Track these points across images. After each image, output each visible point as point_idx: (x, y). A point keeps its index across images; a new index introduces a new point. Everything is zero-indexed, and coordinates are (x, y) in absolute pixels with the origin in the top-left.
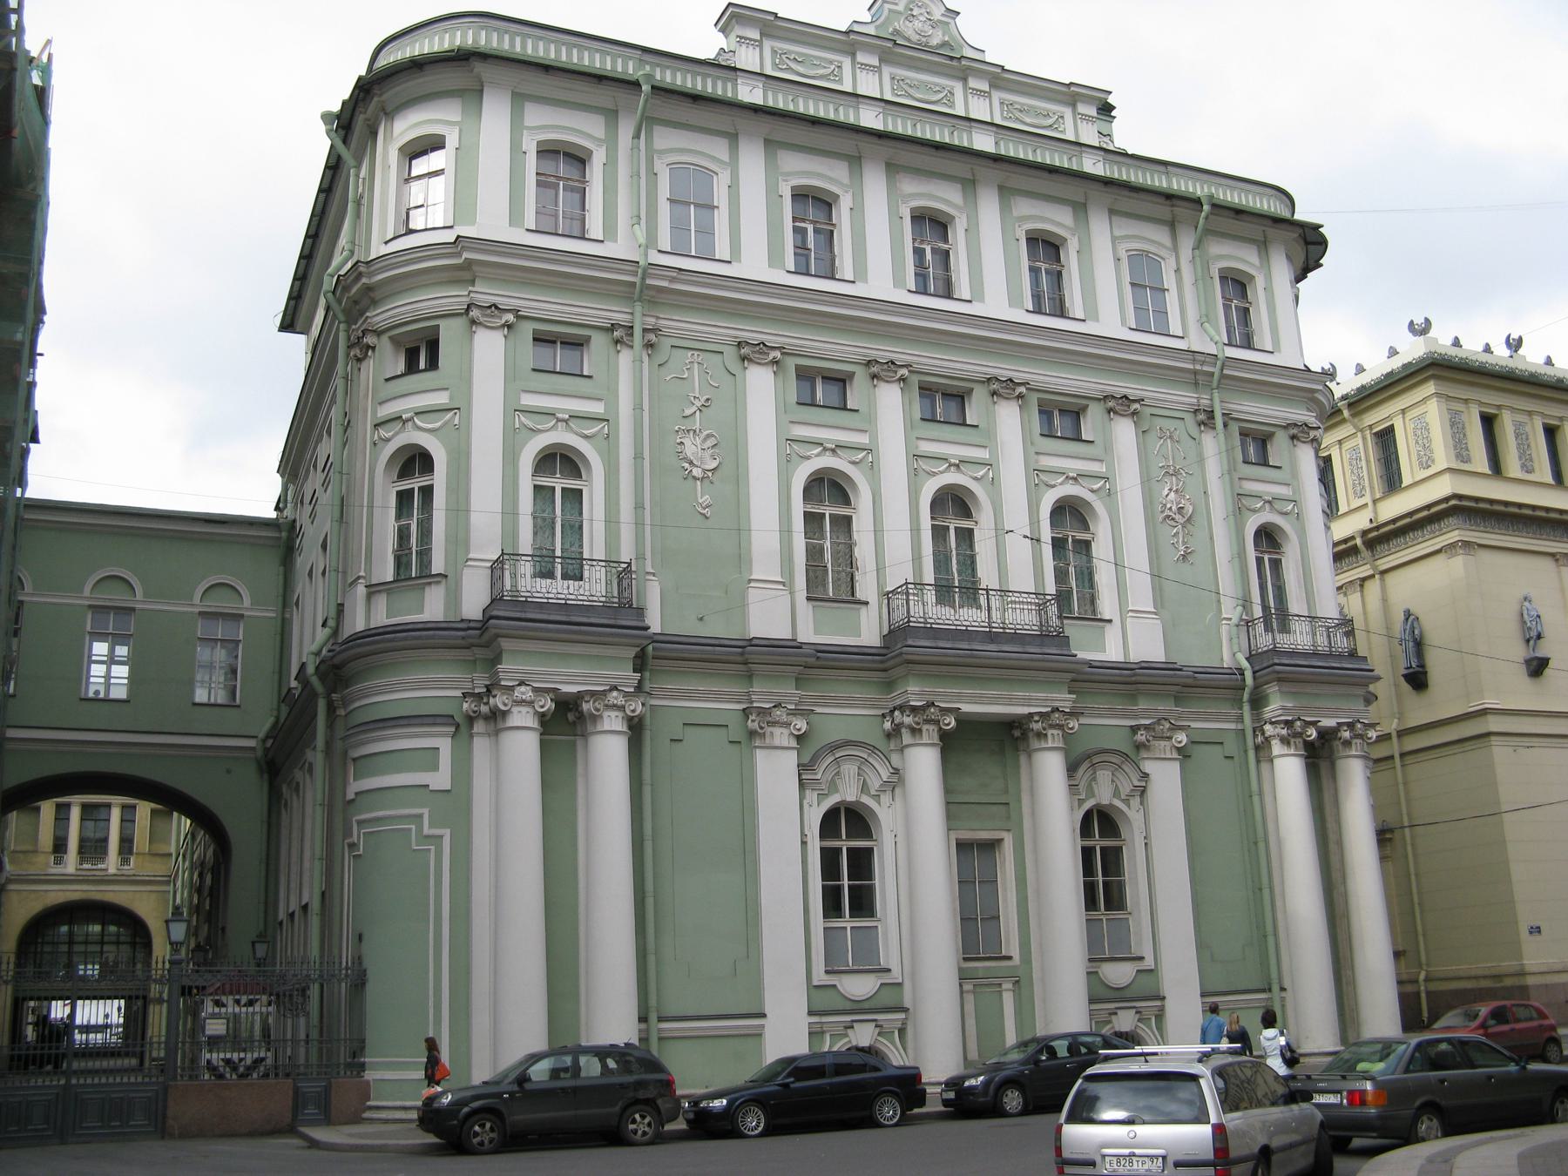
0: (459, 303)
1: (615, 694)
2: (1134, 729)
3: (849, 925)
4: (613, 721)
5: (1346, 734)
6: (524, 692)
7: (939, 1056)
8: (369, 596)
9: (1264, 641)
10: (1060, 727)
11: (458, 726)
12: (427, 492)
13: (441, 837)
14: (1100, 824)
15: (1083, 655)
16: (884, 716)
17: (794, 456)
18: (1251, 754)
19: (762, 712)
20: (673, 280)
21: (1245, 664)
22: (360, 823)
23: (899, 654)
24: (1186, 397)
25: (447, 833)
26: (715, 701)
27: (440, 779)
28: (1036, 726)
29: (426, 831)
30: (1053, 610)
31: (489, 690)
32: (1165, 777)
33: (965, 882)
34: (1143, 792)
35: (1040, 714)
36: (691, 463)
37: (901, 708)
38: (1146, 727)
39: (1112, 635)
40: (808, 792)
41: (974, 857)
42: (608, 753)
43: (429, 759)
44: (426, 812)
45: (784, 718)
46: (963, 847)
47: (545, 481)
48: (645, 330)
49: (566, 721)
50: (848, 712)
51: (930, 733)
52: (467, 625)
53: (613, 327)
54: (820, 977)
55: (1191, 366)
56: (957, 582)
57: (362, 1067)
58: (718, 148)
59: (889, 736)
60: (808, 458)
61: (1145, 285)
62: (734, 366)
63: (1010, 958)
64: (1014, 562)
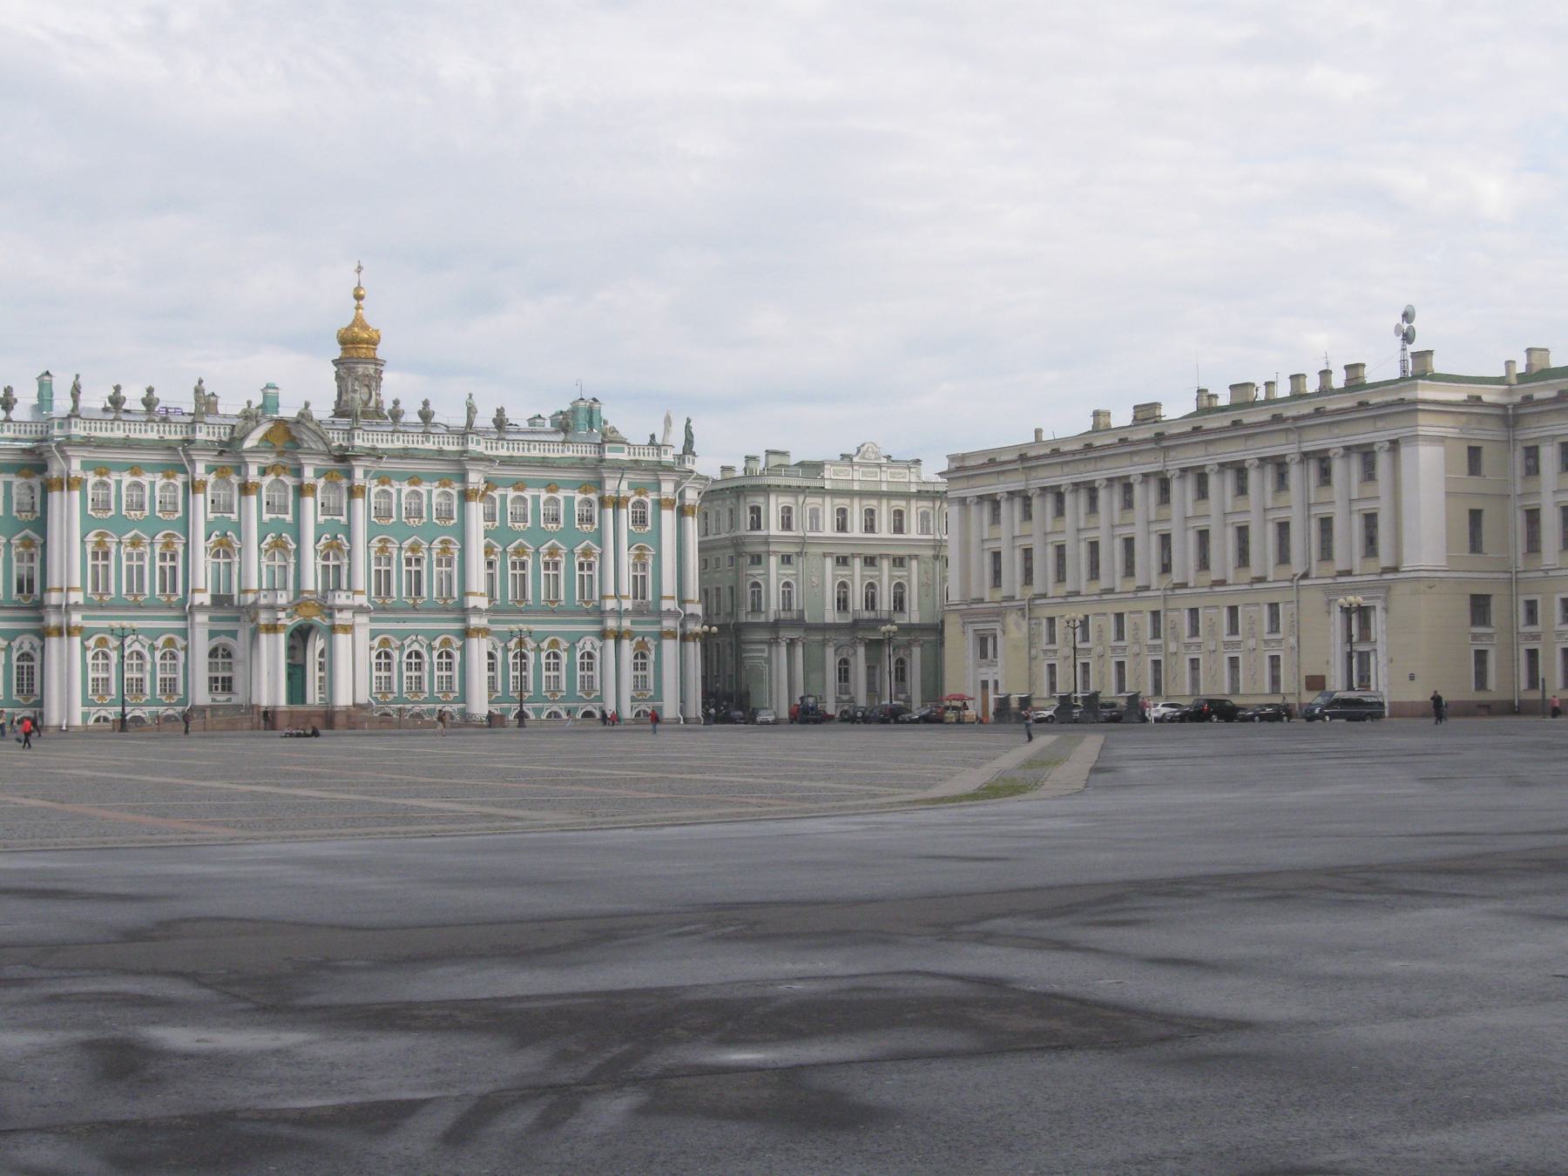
23: (856, 625)
27: (765, 655)
32: (916, 652)
41: (871, 669)
42: (799, 651)
49: (791, 644)
50: (845, 638)
56: (871, 602)
58: (819, 500)
64: (885, 603)
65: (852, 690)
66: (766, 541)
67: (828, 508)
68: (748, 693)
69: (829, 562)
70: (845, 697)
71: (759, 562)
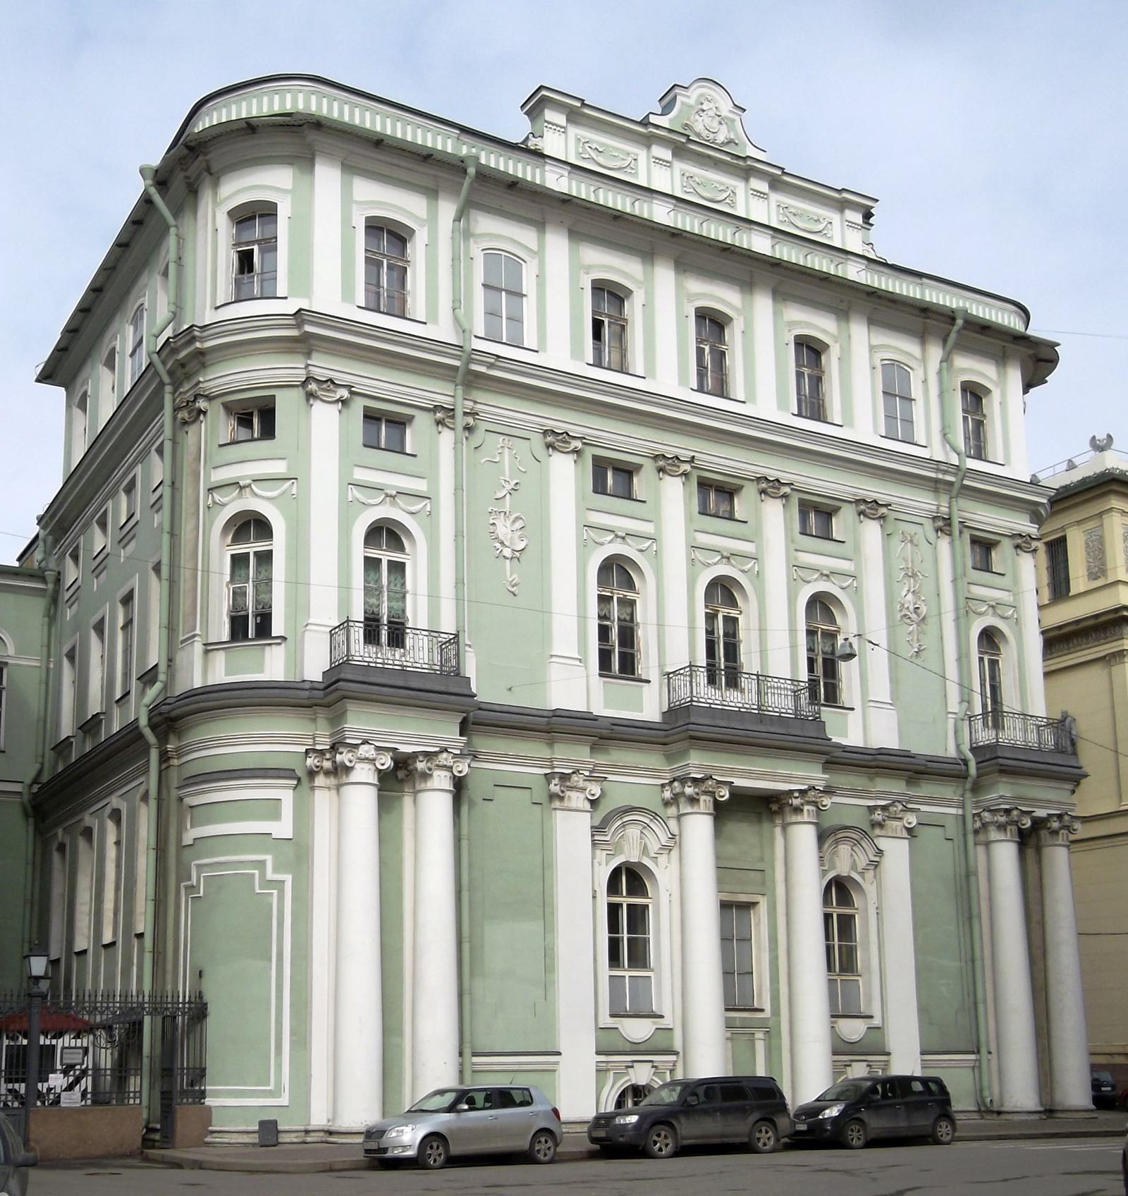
0: (298, 375)
1: (445, 755)
2: (872, 809)
3: (627, 974)
4: (441, 780)
5: (1055, 825)
6: (365, 751)
7: (810, 1080)
8: (206, 652)
9: (985, 736)
10: (815, 803)
11: (299, 780)
12: (265, 558)
13: (283, 882)
14: (839, 890)
15: (835, 739)
16: (663, 786)
17: (590, 543)
18: (970, 837)
19: (564, 777)
20: (491, 366)
21: (970, 756)
22: (198, 866)
24: (925, 502)
25: (288, 878)
26: (517, 763)
27: (283, 828)
28: (796, 802)
29: (270, 875)
30: (804, 697)
31: (334, 748)
32: (896, 852)
33: (726, 939)
34: (876, 865)
35: (800, 791)
36: (502, 543)
37: (683, 780)
38: (884, 808)
39: (854, 719)
40: (598, 852)
43: (271, 809)
44: (269, 858)
45: (581, 784)
46: (725, 906)
47: (374, 553)
48: (465, 414)
51: (706, 802)
52: (313, 687)
53: (436, 408)
54: (606, 1021)
55: (933, 475)
57: (203, 1094)
59: (667, 804)
60: (602, 544)
61: (896, 393)
62: (540, 451)
63: (762, 1010)
64: (776, 650)
65: (664, 999)
66: (304, 336)
67: (558, 275)
68: (199, 1012)
69: (565, 476)
70: (638, 1030)
71: (268, 431)
